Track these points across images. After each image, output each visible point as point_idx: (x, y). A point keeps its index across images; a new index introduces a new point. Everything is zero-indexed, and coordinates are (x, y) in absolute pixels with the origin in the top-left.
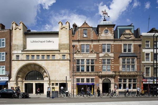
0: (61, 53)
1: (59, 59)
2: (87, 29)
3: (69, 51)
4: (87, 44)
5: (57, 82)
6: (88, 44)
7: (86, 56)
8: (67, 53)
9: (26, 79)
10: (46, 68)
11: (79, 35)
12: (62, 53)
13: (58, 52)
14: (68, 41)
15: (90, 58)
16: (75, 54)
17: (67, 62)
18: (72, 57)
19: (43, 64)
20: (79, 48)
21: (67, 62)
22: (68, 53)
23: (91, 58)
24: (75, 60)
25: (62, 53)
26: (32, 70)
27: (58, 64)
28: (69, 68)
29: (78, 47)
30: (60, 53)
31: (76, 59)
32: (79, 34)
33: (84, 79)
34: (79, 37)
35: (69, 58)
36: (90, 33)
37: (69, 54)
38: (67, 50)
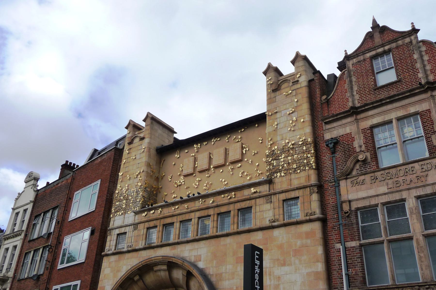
1: (267, 223)
2: (387, 48)
4: (401, 113)
6: (412, 110)
7: (408, 178)
8: (304, 187)
11: (355, 88)
12: (282, 192)
13: (264, 189)
14: (308, 130)
16: (343, 183)
17: (308, 235)
18: (330, 200)
19: (200, 261)
20: (363, 148)
21: (308, 235)
22: (311, 186)
24: (348, 215)
25: (282, 192)
28: (320, 267)
29: (356, 144)
31: (358, 209)
32: (351, 81)
34: (357, 97)
35: (315, 206)
36: (411, 56)
38: (303, 174)
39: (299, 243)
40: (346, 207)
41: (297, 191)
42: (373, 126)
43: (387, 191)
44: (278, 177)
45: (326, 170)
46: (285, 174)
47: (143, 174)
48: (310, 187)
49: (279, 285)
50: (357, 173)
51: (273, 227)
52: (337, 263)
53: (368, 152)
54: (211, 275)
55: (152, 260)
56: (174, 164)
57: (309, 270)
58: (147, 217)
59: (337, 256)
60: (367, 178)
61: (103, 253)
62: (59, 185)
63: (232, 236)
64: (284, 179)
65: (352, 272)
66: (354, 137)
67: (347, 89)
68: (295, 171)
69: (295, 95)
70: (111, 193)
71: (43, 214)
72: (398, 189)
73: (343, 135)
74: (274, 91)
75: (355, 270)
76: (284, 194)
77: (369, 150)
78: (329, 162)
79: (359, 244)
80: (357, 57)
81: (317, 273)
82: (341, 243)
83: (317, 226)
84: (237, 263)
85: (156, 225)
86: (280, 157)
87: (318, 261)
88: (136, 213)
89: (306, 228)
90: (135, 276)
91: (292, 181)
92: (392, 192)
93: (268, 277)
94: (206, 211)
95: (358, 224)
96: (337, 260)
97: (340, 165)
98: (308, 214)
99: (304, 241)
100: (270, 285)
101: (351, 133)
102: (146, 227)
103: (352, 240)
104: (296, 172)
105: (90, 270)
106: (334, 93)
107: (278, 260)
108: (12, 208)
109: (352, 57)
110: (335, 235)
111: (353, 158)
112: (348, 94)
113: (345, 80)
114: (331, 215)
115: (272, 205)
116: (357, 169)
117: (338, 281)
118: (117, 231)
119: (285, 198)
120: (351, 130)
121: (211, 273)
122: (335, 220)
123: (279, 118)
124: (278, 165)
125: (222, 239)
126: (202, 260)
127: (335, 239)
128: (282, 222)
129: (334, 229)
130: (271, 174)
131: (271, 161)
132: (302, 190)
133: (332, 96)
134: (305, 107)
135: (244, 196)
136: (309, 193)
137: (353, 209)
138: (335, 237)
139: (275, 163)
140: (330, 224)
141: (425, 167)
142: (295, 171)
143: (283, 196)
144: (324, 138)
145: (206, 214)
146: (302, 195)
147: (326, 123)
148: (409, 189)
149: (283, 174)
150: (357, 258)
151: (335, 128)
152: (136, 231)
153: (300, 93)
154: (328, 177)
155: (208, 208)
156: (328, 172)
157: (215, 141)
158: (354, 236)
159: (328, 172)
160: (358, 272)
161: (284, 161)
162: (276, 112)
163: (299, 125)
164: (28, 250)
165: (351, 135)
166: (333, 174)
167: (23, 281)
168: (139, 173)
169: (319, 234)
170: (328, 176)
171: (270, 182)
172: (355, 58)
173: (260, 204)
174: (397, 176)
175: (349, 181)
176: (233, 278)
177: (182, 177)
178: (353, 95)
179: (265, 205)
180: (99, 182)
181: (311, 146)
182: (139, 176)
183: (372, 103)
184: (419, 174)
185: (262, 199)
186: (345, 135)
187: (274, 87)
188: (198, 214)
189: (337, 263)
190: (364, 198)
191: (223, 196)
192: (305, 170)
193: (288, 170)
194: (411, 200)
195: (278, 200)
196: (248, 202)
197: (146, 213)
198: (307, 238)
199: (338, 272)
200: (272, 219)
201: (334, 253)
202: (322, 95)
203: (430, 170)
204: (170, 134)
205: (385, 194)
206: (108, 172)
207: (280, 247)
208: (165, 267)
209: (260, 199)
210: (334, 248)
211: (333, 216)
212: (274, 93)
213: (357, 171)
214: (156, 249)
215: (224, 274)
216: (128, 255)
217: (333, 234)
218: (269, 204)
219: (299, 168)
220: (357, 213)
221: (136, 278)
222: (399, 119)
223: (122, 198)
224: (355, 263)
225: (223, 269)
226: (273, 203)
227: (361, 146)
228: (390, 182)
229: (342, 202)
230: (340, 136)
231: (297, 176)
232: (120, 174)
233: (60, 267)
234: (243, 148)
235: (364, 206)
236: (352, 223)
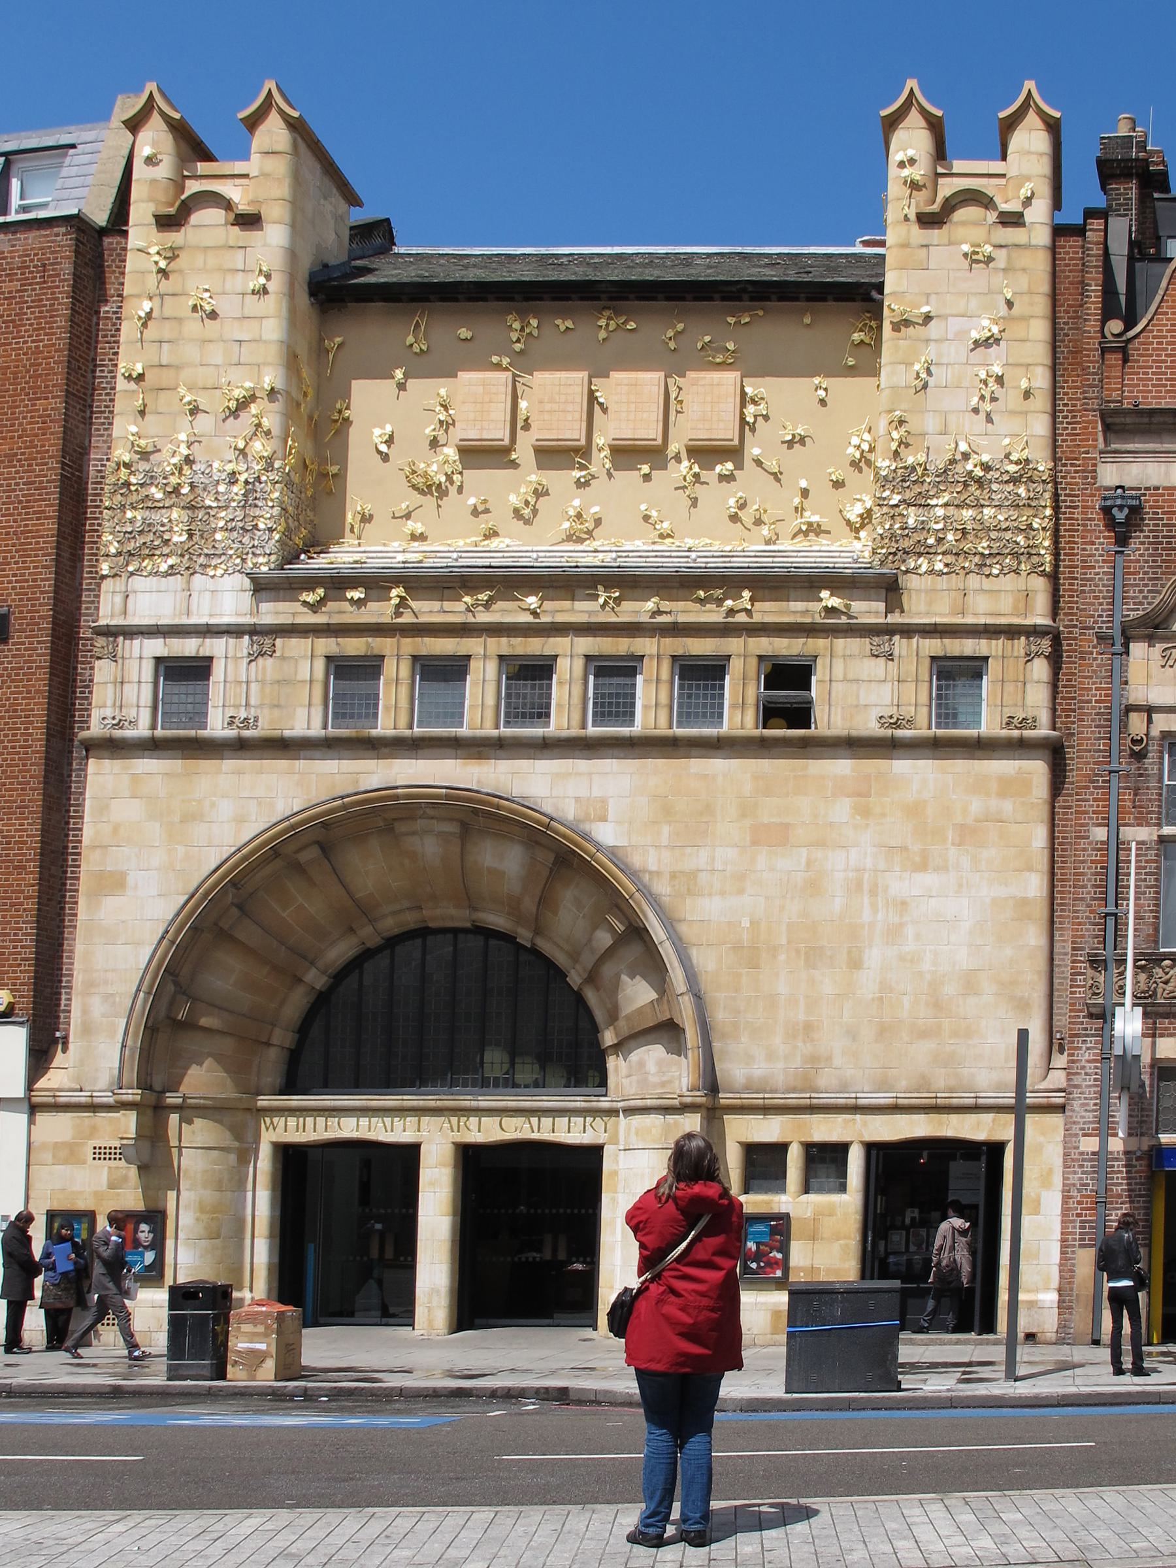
0: (907, 631)
3: (1040, 584)
8: (1011, 632)
10: (662, 888)
17: (1006, 787)
19: (604, 819)
26: (411, 920)
28: (1035, 885)
30: (889, 631)
35: (1037, 700)
37: (1045, 644)
39: (976, 806)
45: (1090, 592)
46: (947, 565)
49: (902, 925)
52: (1090, 880)
54: (651, 873)
64: (942, 582)
68: (981, 566)
78: (1103, 567)
79: (1159, 836)
81: (1024, 902)
84: (755, 843)
86: (933, 502)
87: (1030, 869)
91: (970, 598)
93: (866, 901)
95: (1161, 780)
96: (1092, 874)
99: (994, 803)
103: (1141, 822)
104: (986, 571)
106: (1148, 325)
107: (904, 849)
110: (1095, 800)
114: (1090, 739)
119: (941, 654)
121: (653, 868)
123: (936, 341)
124: (923, 528)
126: (610, 818)
130: (895, 554)
133: (1141, 332)
136: (1022, 653)
140: (1078, 767)
142: (981, 566)
146: (1000, 653)
149: (939, 566)
150: (1146, 874)
156: (1096, 598)
158: (1149, 813)
159: (1096, 598)
160: (1145, 912)
163: (1010, 398)
166: (1110, 610)
173: (848, 653)
176: (741, 891)
181: (1044, 491)
189: (1090, 880)
192: (1016, 572)
193: (957, 554)
195: (917, 655)
198: (1002, 794)
199: (1088, 906)
200: (891, 717)
201: (1086, 853)
207: (914, 811)
210: (1088, 837)
215: (703, 876)
217: (1087, 797)
218: (882, 661)
219: (998, 557)
225: (698, 859)
226: (896, 661)
231: (987, 584)
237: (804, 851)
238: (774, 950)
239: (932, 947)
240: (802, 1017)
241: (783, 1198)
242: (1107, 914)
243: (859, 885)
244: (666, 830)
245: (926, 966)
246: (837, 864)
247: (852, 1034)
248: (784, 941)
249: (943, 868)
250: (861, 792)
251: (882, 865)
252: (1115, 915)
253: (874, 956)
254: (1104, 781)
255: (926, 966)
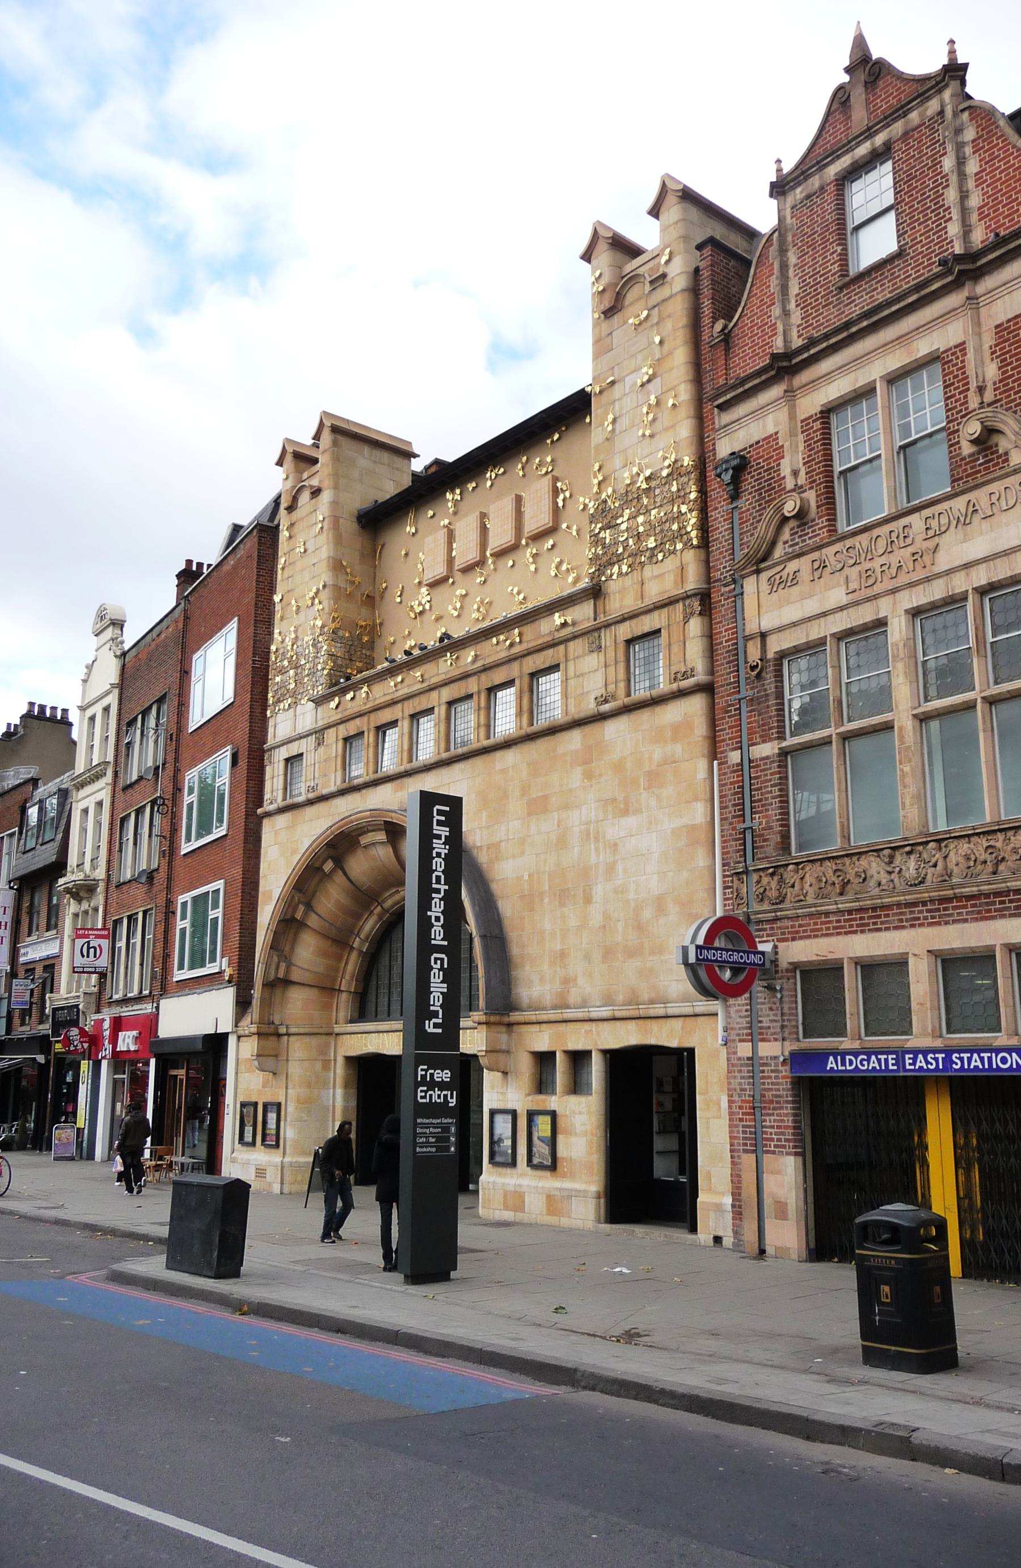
2: (879, 139)
4: (895, 361)
5: (577, 1039)
6: (923, 347)
7: (894, 559)
8: (669, 603)
9: (371, 1007)
11: (794, 289)
12: (623, 619)
13: (583, 613)
14: (685, 430)
15: (960, 583)
16: (750, 585)
20: (802, 479)
21: (678, 731)
23: (981, 577)
25: (623, 619)
27: (589, 776)
32: (784, 267)
33: (899, 965)
35: (695, 655)
36: (937, 163)
38: (671, 564)
39: (658, 754)
40: (754, 653)
41: (656, 614)
42: (829, 406)
43: (844, 600)
44: (614, 577)
47: (324, 595)
48: (684, 599)
49: (615, 862)
50: (783, 552)
51: (601, 717)
52: (730, 800)
53: (811, 488)
54: (477, 848)
55: (353, 822)
56: (407, 555)
57: (678, 822)
58: (339, 709)
59: (731, 783)
60: (803, 565)
61: (259, 811)
62: (163, 636)
63: (519, 745)
64: (628, 581)
65: (760, 824)
66: (782, 446)
67: (774, 293)
68: (651, 557)
69: (657, 324)
70: (263, 652)
71: (140, 717)
72: (870, 592)
73: (758, 443)
74: (609, 313)
75: (766, 816)
76: (627, 623)
77: (814, 481)
80: (806, 179)
81: (693, 828)
82: (741, 748)
83: (697, 704)
84: (529, 814)
85: (361, 730)
86: (619, 521)
88: (319, 701)
89: (673, 713)
90: (325, 861)
91: (646, 586)
92: (856, 604)
94: (463, 683)
97: (748, 531)
98: (679, 676)
100: (597, 865)
101: (776, 433)
102: (341, 736)
104: (654, 560)
105: (239, 853)
106: (743, 311)
108: (78, 707)
109: (792, 184)
110: (730, 728)
111: (772, 511)
112: (776, 311)
113: (772, 264)
115: (602, 655)
116: (785, 543)
117: (731, 846)
118: (283, 753)
119: (630, 637)
120: (776, 424)
121: (478, 844)
122: (730, 689)
123: (618, 400)
125: (498, 754)
127: (730, 739)
128: (622, 700)
129: (728, 712)
130: (599, 569)
131: (599, 533)
132: (666, 610)
133: (738, 320)
134: (680, 357)
135: (541, 636)
137: (770, 655)
138: (728, 734)
139: (607, 535)
141: (934, 524)
142: (651, 557)
143: (625, 631)
144: (715, 454)
145: (462, 693)
147: (723, 407)
148: (894, 591)
150: (772, 786)
151: (740, 422)
152: (321, 749)
153: (669, 316)
154: (719, 570)
155: (465, 676)
157: (493, 477)
158: (770, 729)
160: (773, 822)
161: (627, 529)
162: (613, 383)
163: (665, 418)
164: (124, 810)
165: (777, 438)
167: (125, 888)
168: (317, 593)
169: (700, 729)
170: (722, 568)
171: (595, 592)
172: (799, 184)
174: (869, 557)
175: (764, 576)
176: (523, 853)
177: (424, 590)
178: (786, 313)
179: (586, 657)
180: (234, 624)
181: (689, 480)
182: (317, 601)
183: (826, 337)
184: (920, 545)
185: (579, 642)
186: (763, 440)
187: (607, 304)
188: (446, 694)
190: (794, 624)
191: (494, 640)
193: (636, 555)
194: (896, 621)
196: (551, 651)
197: (337, 699)
198: (675, 740)
199: (731, 824)
200: (602, 696)
201: (726, 777)
202: (715, 320)
203: (945, 532)
204: (399, 461)
205: (842, 608)
206: (250, 597)
207: (619, 767)
208: (382, 836)
209: (576, 641)
211: (727, 679)
212: (607, 321)
213: (785, 548)
214: (364, 791)
216: (310, 811)
218: (595, 655)
220: (781, 665)
221: (328, 866)
222: (893, 379)
223: (286, 663)
224: (766, 799)
227: (795, 473)
228: (853, 573)
229: (747, 639)
230: (750, 446)
232: (277, 598)
233: (185, 848)
234: (556, 492)
235: (794, 647)
236: (767, 695)
237: (556, 814)
238: (542, 895)
239: (634, 879)
240: (559, 947)
241: (554, 1098)
242: (745, 829)
243: (588, 835)
244: (484, 814)
245: (631, 896)
246: (575, 819)
247: (588, 957)
248: (547, 888)
249: (638, 811)
250: (587, 759)
251: (601, 816)
252: (751, 828)
253: (599, 891)
254: (735, 710)
255: (631, 896)
